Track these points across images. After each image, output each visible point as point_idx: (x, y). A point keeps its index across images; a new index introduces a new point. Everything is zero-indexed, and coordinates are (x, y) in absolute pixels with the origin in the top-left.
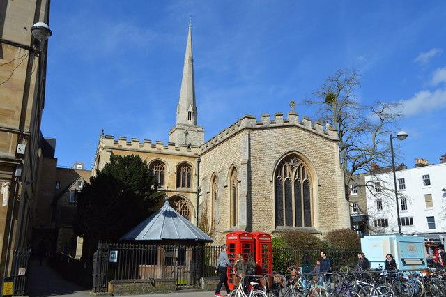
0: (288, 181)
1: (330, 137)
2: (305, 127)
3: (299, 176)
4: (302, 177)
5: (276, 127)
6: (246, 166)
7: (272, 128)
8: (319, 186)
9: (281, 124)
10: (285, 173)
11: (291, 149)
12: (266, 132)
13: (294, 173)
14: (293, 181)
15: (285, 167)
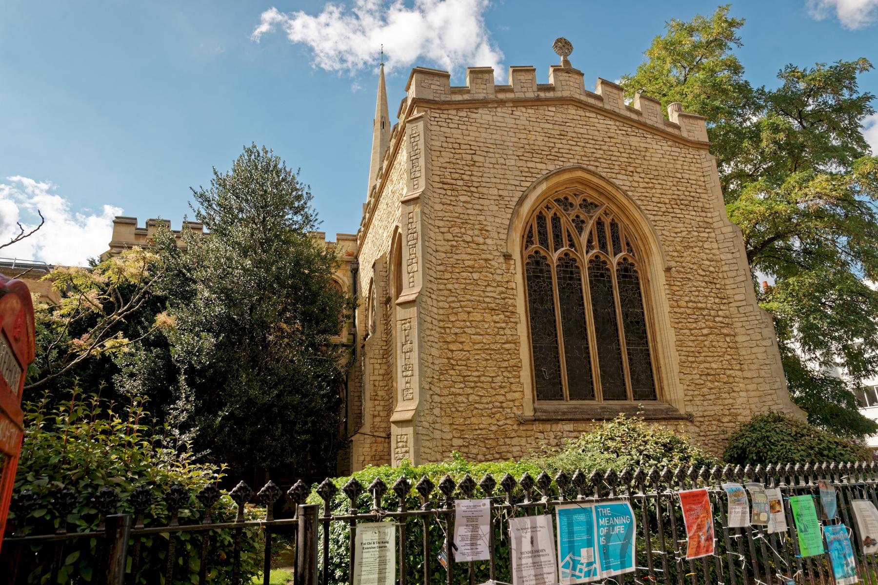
1: (685, 134)
2: (607, 107)
3: (603, 246)
4: (610, 247)
5: (518, 103)
7: (502, 103)
8: (668, 270)
9: (531, 95)
10: (557, 237)
12: (483, 115)
13: (584, 238)
14: (585, 259)
15: (556, 220)
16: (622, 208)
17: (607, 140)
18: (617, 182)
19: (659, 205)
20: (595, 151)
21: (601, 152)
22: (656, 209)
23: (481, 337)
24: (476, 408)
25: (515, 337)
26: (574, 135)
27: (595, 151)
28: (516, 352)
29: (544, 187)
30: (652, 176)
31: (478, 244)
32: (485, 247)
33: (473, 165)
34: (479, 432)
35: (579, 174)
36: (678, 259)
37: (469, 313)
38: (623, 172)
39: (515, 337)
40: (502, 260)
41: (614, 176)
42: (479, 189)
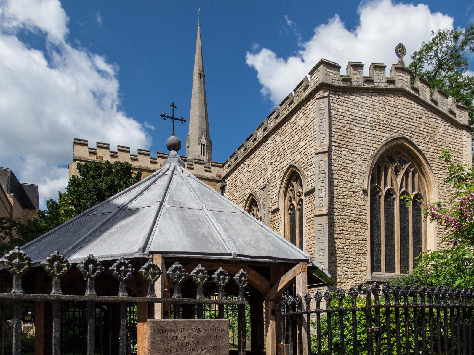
0: (390, 194)
1: (457, 119)
6: (325, 158)
11: (397, 135)
12: (357, 99)
13: (399, 180)
14: (398, 193)
16: (420, 164)
17: (418, 119)
18: (420, 148)
19: (439, 164)
20: (410, 126)
21: (414, 127)
22: (437, 166)
23: (349, 236)
24: (346, 274)
25: (365, 237)
26: (402, 115)
27: (410, 126)
28: (364, 246)
29: (384, 149)
30: (437, 145)
31: (350, 182)
32: (353, 184)
33: (350, 131)
34: (347, 286)
35: (402, 141)
36: (444, 197)
37: (345, 222)
38: (423, 141)
39: (365, 237)
40: (361, 192)
41: (419, 143)
42: (353, 147)
